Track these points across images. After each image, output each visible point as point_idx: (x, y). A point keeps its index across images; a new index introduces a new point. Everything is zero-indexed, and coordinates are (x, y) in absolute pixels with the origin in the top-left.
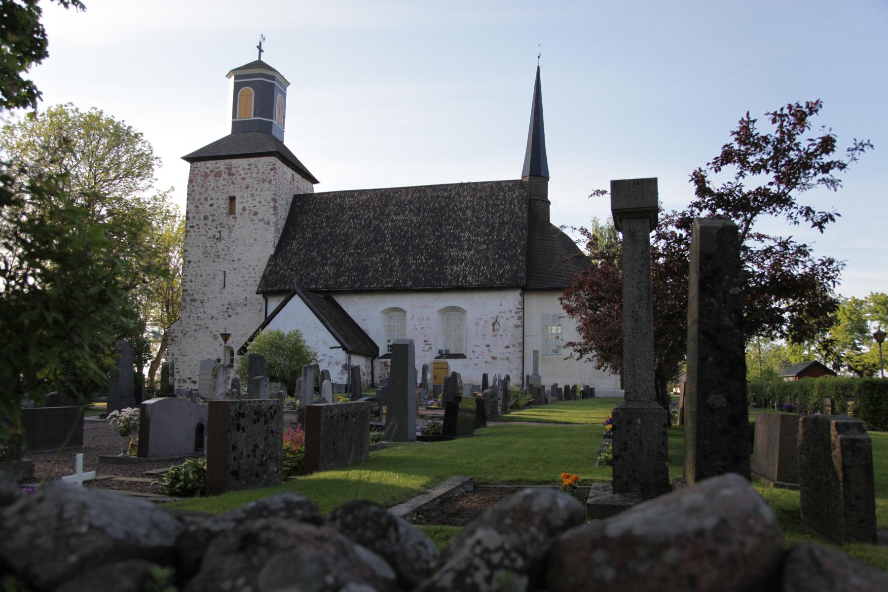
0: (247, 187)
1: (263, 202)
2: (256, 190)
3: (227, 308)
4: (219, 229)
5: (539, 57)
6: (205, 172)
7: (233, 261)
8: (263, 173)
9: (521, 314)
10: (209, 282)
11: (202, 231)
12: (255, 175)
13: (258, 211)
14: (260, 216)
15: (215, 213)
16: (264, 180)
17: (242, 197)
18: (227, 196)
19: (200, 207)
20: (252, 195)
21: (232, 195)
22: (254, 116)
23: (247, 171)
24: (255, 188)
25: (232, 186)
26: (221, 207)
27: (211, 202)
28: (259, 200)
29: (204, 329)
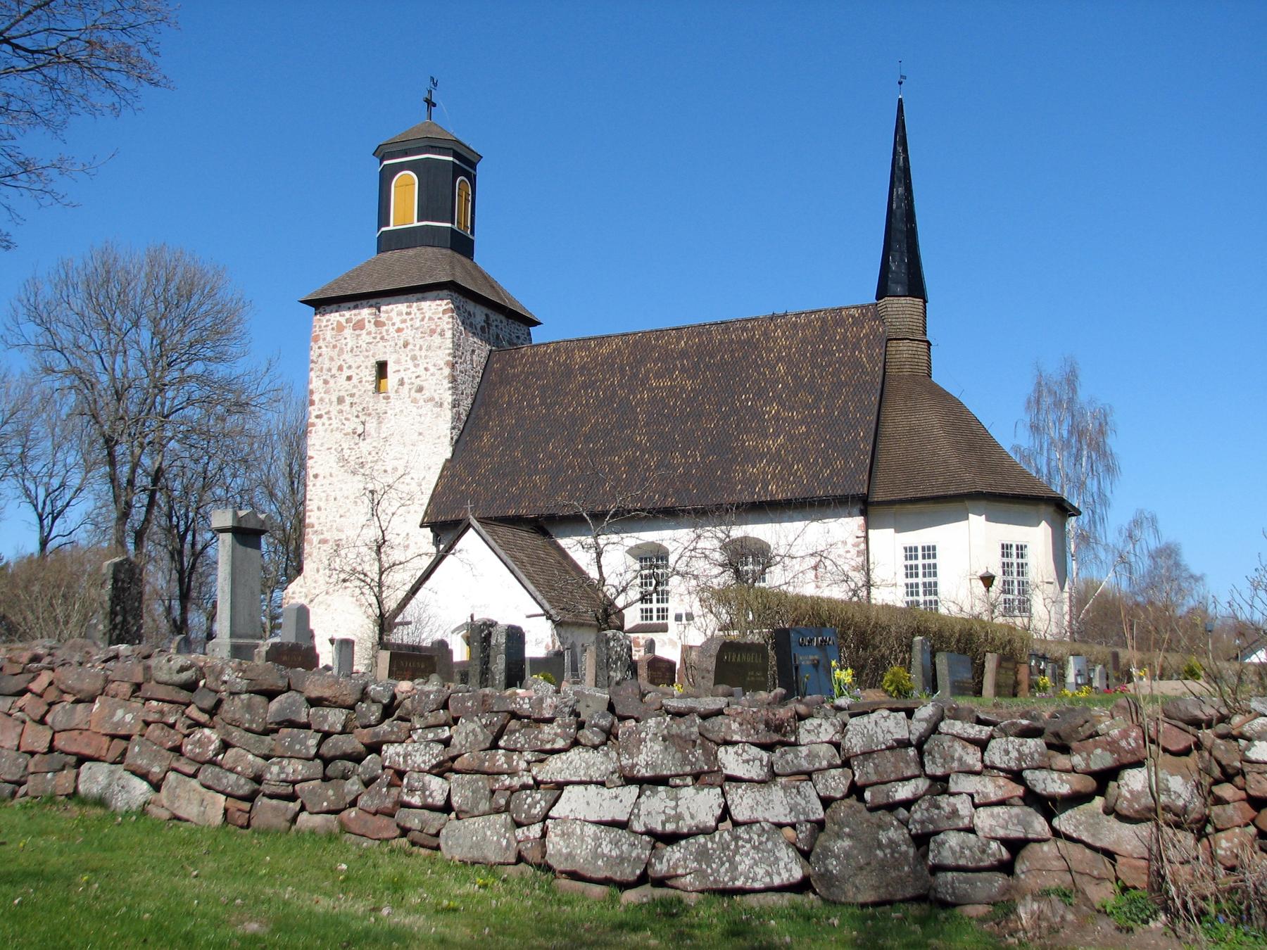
0: (406, 345)
1: (432, 369)
2: (421, 349)
4: (363, 418)
5: (900, 83)
6: (338, 322)
7: (385, 471)
8: (430, 319)
9: (863, 546)
10: (349, 510)
11: (335, 423)
12: (418, 324)
13: (424, 384)
14: (426, 394)
15: (354, 391)
16: (433, 332)
17: (398, 362)
18: (373, 361)
19: (332, 381)
20: (414, 358)
21: (381, 358)
22: (418, 221)
23: (405, 317)
24: (418, 346)
25: (381, 344)
26: (364, 379)
27: (349, 373)
28: (425, 365)
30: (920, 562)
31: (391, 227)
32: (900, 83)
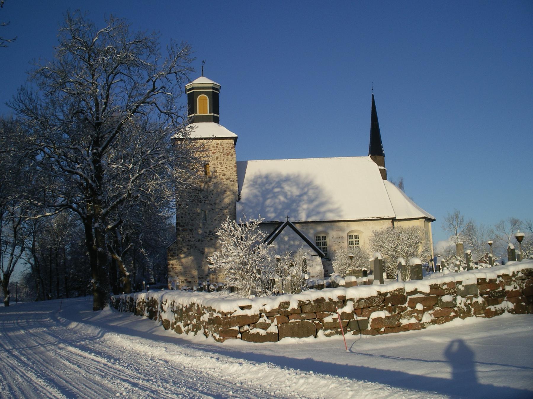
0: (217, 158)
1: (229, 168)
2: (223, 160)
3: (209, 234)
5: (373, 89)
8: (226, 150)
12: (221, 151)
13: (226, 173)
16: (228, 155)
20: (221, 163)
23: (215, 148)
24: (222, 159)
29: (194, 248)
30: (354, 240)
31: (198, 114)
32: (373, 89)
